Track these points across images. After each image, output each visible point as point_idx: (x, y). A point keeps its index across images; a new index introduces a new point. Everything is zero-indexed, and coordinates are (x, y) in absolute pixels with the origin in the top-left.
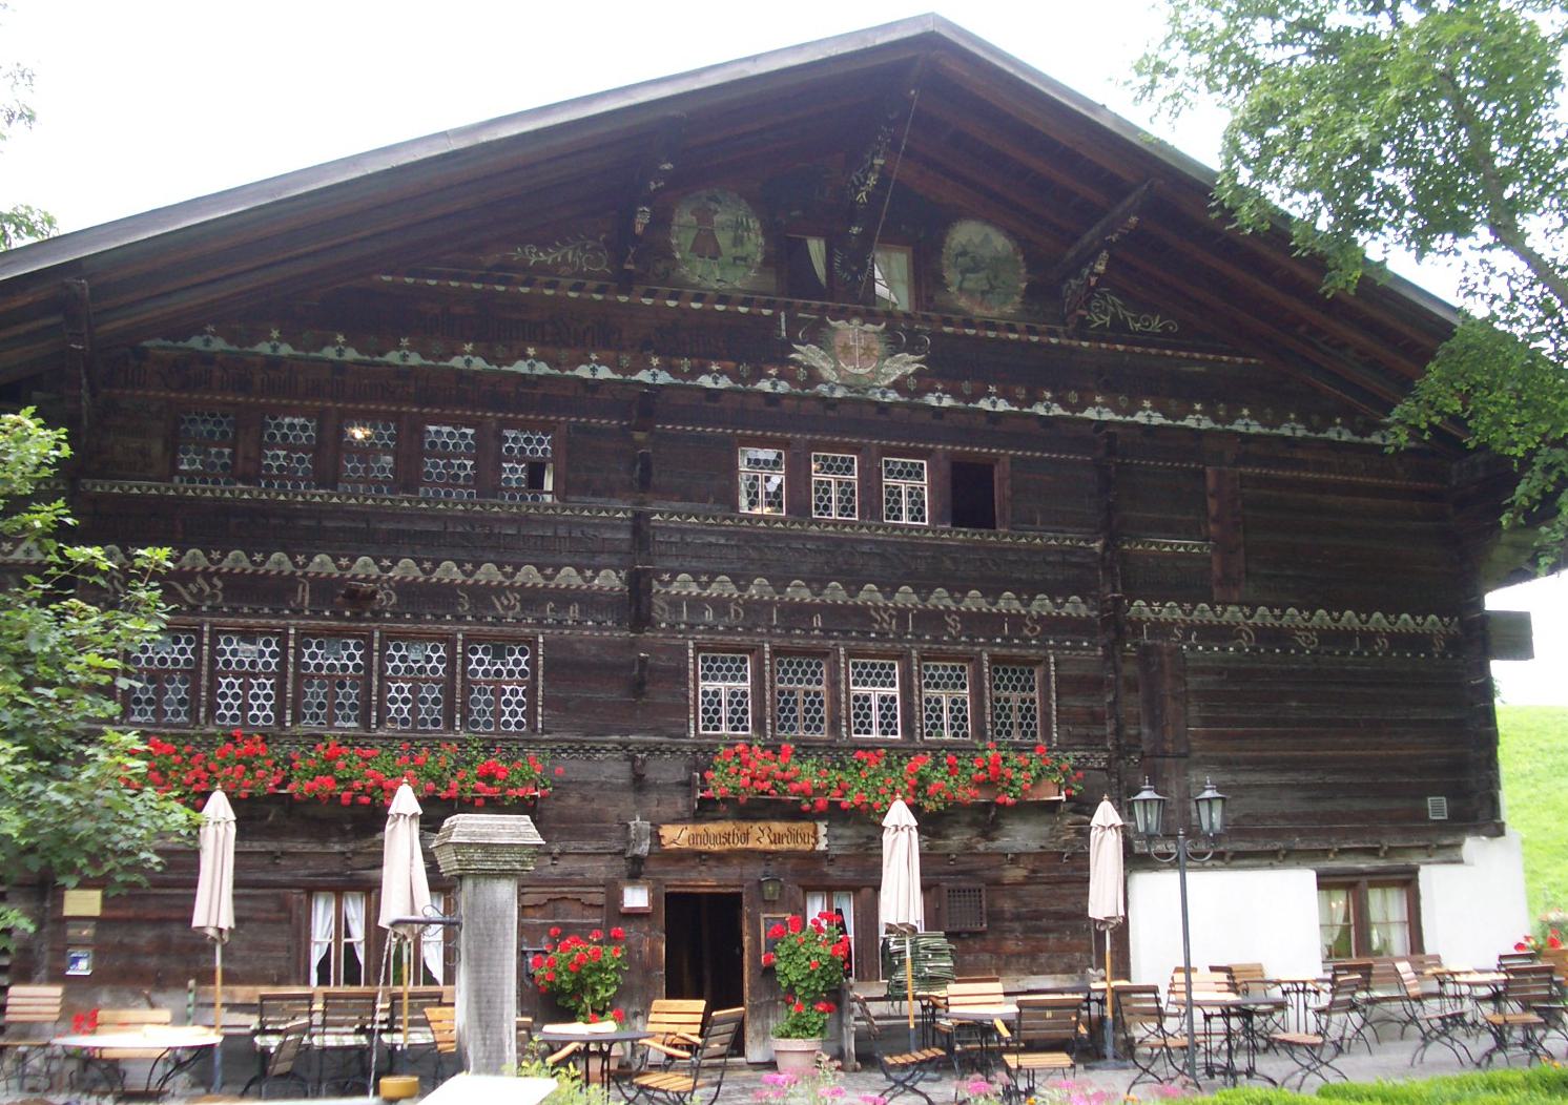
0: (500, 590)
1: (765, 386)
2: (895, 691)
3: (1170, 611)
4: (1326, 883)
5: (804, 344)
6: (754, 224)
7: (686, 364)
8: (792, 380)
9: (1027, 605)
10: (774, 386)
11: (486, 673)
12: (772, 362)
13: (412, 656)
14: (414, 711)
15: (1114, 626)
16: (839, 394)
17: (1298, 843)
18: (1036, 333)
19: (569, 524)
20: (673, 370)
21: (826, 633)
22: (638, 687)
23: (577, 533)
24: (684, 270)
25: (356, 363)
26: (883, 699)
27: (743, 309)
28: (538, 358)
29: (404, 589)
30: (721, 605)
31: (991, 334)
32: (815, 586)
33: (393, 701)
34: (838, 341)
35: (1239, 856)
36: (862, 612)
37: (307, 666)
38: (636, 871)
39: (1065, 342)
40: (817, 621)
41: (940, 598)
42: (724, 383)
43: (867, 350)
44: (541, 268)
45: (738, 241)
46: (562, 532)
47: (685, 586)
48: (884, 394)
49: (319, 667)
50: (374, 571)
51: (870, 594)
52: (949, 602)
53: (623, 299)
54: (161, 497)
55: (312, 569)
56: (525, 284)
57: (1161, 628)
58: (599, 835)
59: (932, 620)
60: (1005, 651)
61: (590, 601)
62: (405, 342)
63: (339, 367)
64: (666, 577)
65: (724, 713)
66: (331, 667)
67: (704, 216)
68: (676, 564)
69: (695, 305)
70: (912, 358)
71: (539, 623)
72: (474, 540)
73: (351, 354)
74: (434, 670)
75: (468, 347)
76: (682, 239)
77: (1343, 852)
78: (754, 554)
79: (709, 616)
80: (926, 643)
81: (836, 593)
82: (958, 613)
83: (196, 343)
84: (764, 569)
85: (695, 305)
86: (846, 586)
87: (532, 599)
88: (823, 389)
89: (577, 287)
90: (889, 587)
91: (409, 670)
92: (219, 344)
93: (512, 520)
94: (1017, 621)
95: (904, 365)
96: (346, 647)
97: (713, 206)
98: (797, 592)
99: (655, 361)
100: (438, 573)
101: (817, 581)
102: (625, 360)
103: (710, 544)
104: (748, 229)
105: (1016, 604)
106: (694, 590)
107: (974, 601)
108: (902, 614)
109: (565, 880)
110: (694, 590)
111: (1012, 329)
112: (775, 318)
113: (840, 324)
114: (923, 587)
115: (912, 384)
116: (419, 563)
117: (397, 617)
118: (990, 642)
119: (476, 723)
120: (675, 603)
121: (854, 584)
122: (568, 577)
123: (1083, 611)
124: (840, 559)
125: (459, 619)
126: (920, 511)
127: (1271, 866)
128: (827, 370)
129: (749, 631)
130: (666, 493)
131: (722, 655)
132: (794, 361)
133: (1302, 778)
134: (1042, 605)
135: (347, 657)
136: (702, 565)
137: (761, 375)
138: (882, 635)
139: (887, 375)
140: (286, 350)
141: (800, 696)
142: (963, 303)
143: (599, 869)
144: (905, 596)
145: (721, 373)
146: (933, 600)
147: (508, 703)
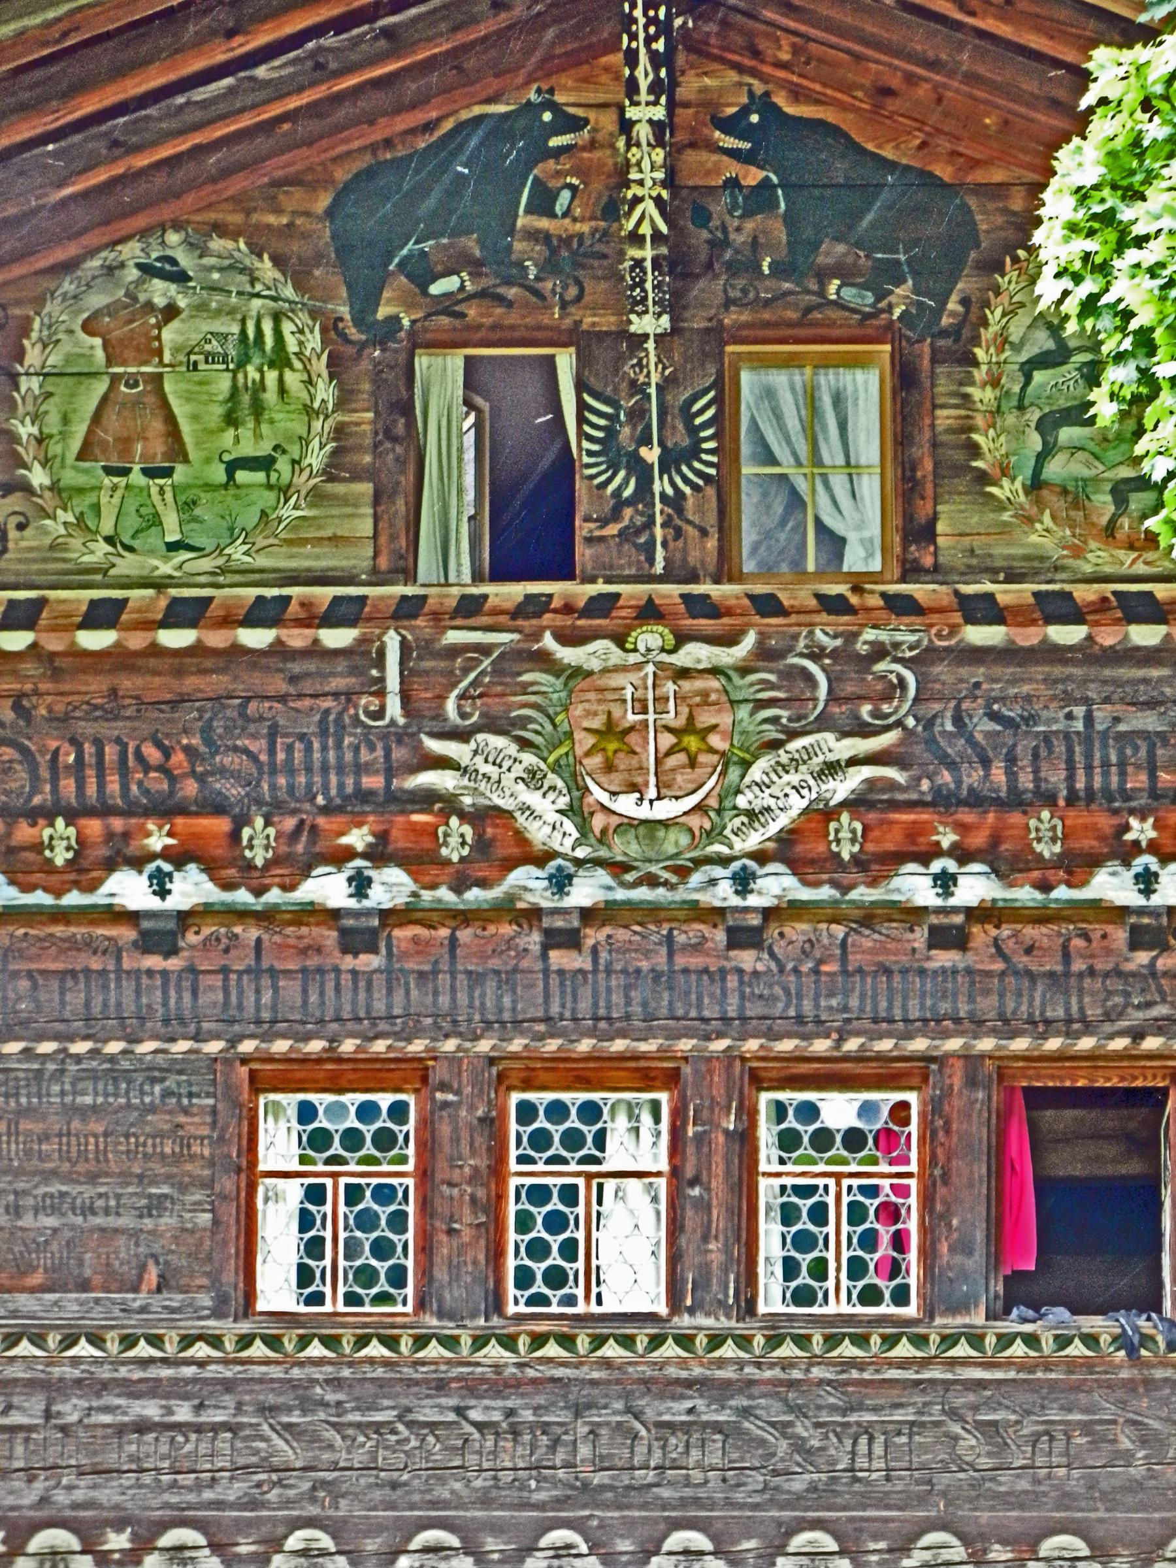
5: (461, 735)
8: (421, 860)
16: (586, 891)
48: (743, 883)
67: (130, 334)
76: (51, 417)
78: (286, 1451)
88: (528, 881)
103: (142, 1427)
112: (366, 656)
128: (545, 819)
136: (109, 1494)
145: (179, 858)
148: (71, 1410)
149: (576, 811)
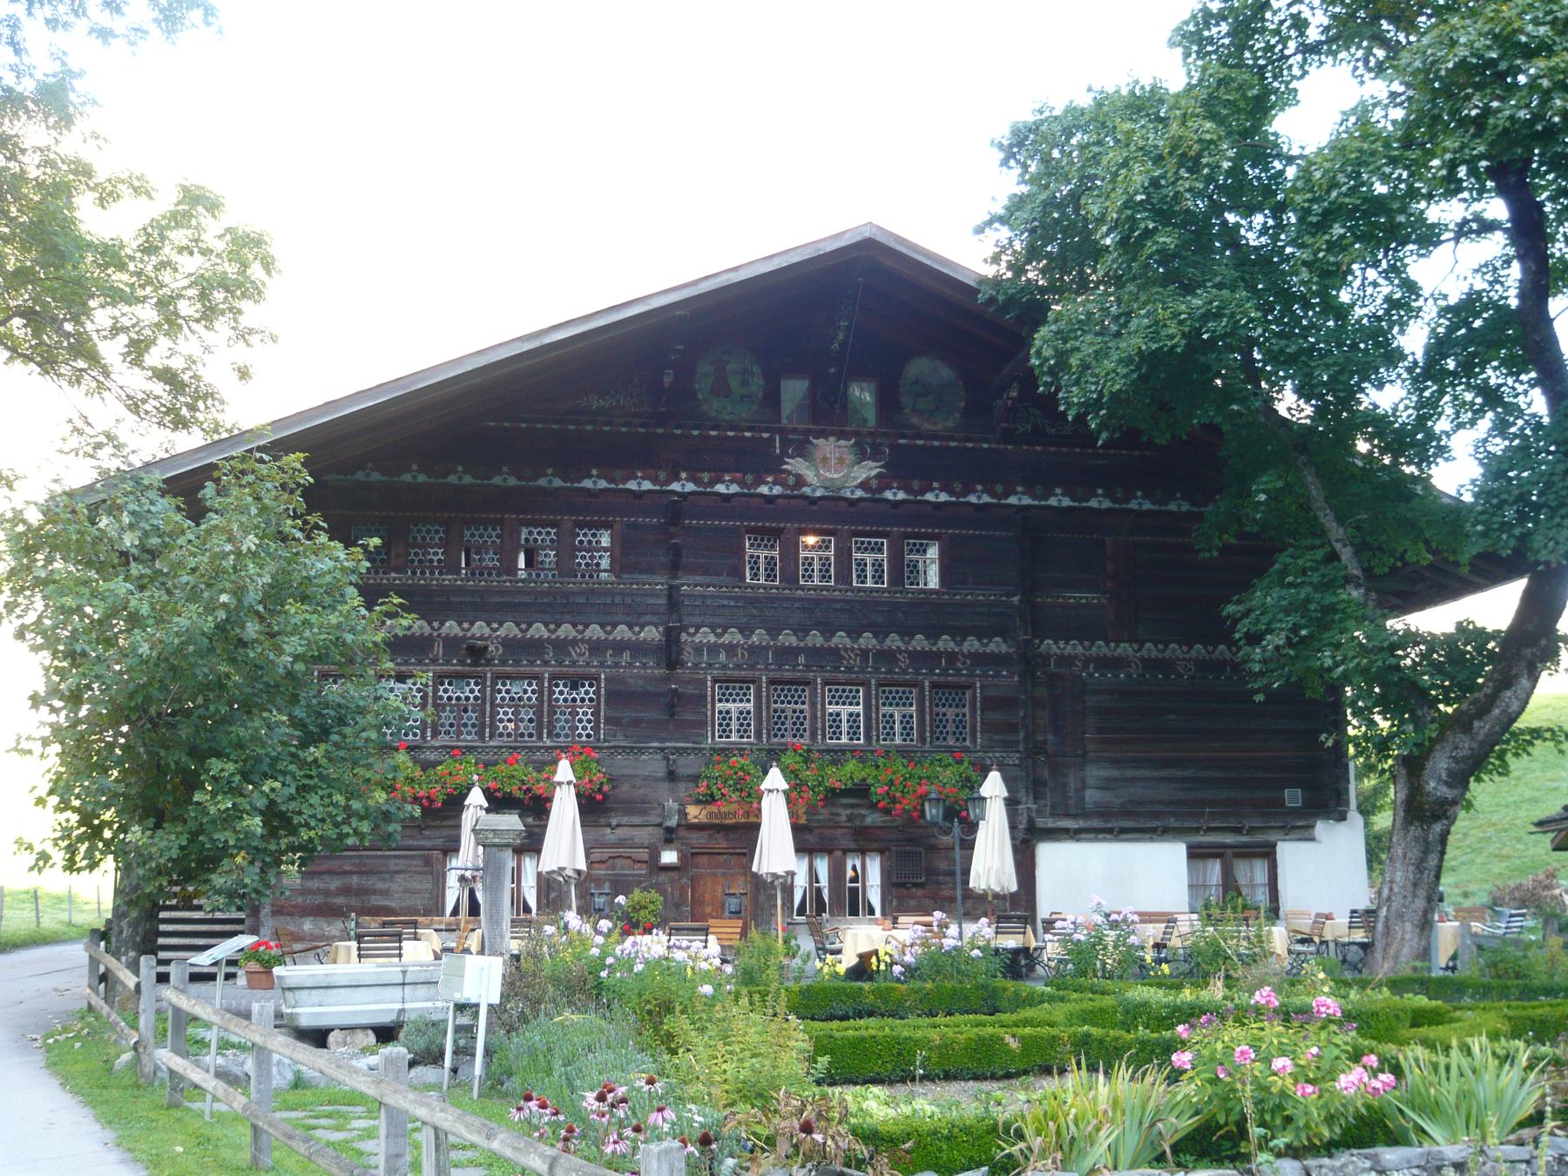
0: (574, 642)
1: (764, 490)
2: (860, 709)
3: (1073, 648)
4: (1195, 854)
6: (757, 370)
7: (706, 477)
8: (784, 484)
9: (959, 644)
10: (771, 489)
11: (565, 700)
12: (770, 472)
13: (514, 690)
14: (517, 727)
15: (1029, 662)
16: (818, 494)
17: (1173, 823)
18: (970, 440)
19: (623, 594)
20: (697, 482)
21: (808, 667)
22: (671, 709)
24: (705, 407)
25: (472, 485)
26: (851, 715)
27: (748, 434)
28: (599, 477)
29: (508, 643)
30: (731, 649)
31: (936, 443)
33: (501, 721)
34: (818, 455)
35: (1123, 831)
36: (835, 653)
37: (441, 698)
38: (670, 837)
39: (994, 446)
40: (802, 659)
41: (894, 641)
42: (734, 489)
43: (841, 460)
45: (745, 383)
46: (618, 600)
47: (706, 636)
49: (450, 698)
50: (487, 631)
51: (840, 639)
52: (900, 644)
53: (660, 431)
55: (444, 631)
56: (590, 423)
57: (1065, 660)
58: (643, 812)
59: (888, 656)
60: (942, 679)
61: (638, 649)
62: (505, 469)
63: (459, 489)
64: (692, 630)
65: (734, 725)
66: (458, 698)
68: (698, 620)
69: (713, 433)
70: (871, 464)
71: (602, 665)
72: (556, 606)
73: (468, 479)
74: (529, 699)
75: (550, 471)
77: (1210, 830)
78: (755, 612)
79: (722, 657)
80: (884, 676)
81: (815, 639)
82: (907, 651)
83: (360, 475)
84: (763, 623)
85: (713, 433)
86: (823, 634)
87: (596, 647)
88: (806, 490)
90: (854, 633)
92: (376, 476)
93: (582, 593)
94: (952, 657)
95: (868, 470)
96: (468, 684)
98: (788, 639)
99: (684, 475)
101: (801, 631)
102: (662, 475)
105: (952, 644)
106: (712, 638)
107: (919, 642)
108: (864, 653)
109: (620, 844)
110: (712, 638)
111: (952, 439)
112: (771, 439)
113: (821, 441)
114: (880, 632)
115: (874, 484)
116: (518, 625)
117: (503, 663)
119: (558, 735)
120: (698, 649)
121: (829, 633)
122: (622, 632)
123: (1004, 648)
124: (820, 613)
125: (546, 663)
126: (881, 577)
127: (1152, 840)
128: (810, 476)
129: (752, 667)
130: (693, 570)
131: (733, 683)
132: (785, 471)
133: (1179, 773)
134: (972, 644)
135: (470, 691)
136: (717, 620)
137: (760, 481)
138: (849, 670)
139: (855, 478)
140: (422, 478)
141: (789, 714)
142: (915, 420)
143: (644, 835)
144: (867, 640)
145: (732, 482)
146: (888, 642)
147: (580, 721)
148: (708, 602)
149: (818, 475)
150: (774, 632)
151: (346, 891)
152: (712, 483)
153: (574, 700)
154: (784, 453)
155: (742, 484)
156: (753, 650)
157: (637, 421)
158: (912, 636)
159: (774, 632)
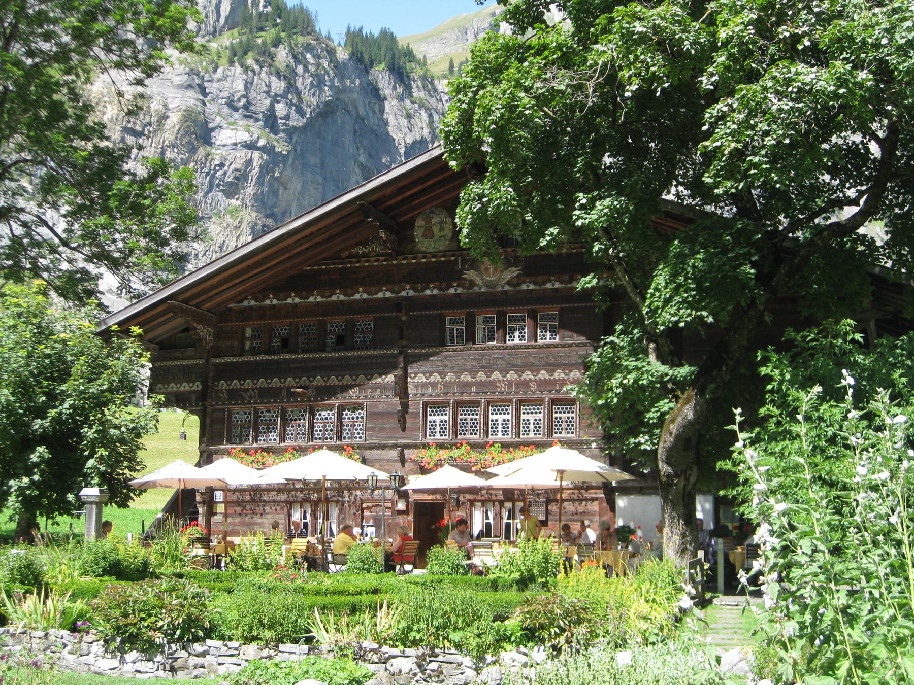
8: (463, 287)
11: (349, 418)
14: (324, 434)
16: (483, 290)
18: (574, 248)
23: (379, 361)
26: (504, 420)
27: (443, 259)
28: (363, 292)
30: (434, 385)
32: (473, 374)
34: (483, 267)
36: (493, 384)
40: (474, 389)
41: (528, 375)
44: (364, 255)
45: (442, 229)
51: (496, 375)
52: (531, 377)
53: (395, 262)
54: (237, 362)
62: (315, 292)
65: (438, 429)
67: (428, 220)
70: (515, 269)
75: (338, 291)
76: (418, 234)
79: (430, 390)
81: (481, 376)
82: (535, 380)
83: (245, 303)
85: (423, 260)
88: (476, 289)
89: (377, 261)
91: (322, 419)
92: (253, 303)
95: (512, 273)
97: (431, 215)
98: (466, 377)
99: (408, 287)
100: (329, 381)
104: (446, 223)
105: (563, 375)
106: (424, 380)
107: (543, 375)
108: (510, 383)
110: (424, 380)
112: (456, 261)
118: (550, 391)
119: (345, 438)
126: (523, 336)
128: (478, 280)
129: (446, 394)
132: (464, 279)
137: (449, 286)
141: (469, 421)
144: (512, 375)
146: (524, 376)
147: (356, 430)
149: (482, 279)
150: (458, 374)
151: (242, 524)
152: (423, 290)
153: (353, 418)
154: (463, 268)
155: (440, 289)
156: (446, 385)
157: (382, 258)
158: (538, 371)
159: (458, 374)
